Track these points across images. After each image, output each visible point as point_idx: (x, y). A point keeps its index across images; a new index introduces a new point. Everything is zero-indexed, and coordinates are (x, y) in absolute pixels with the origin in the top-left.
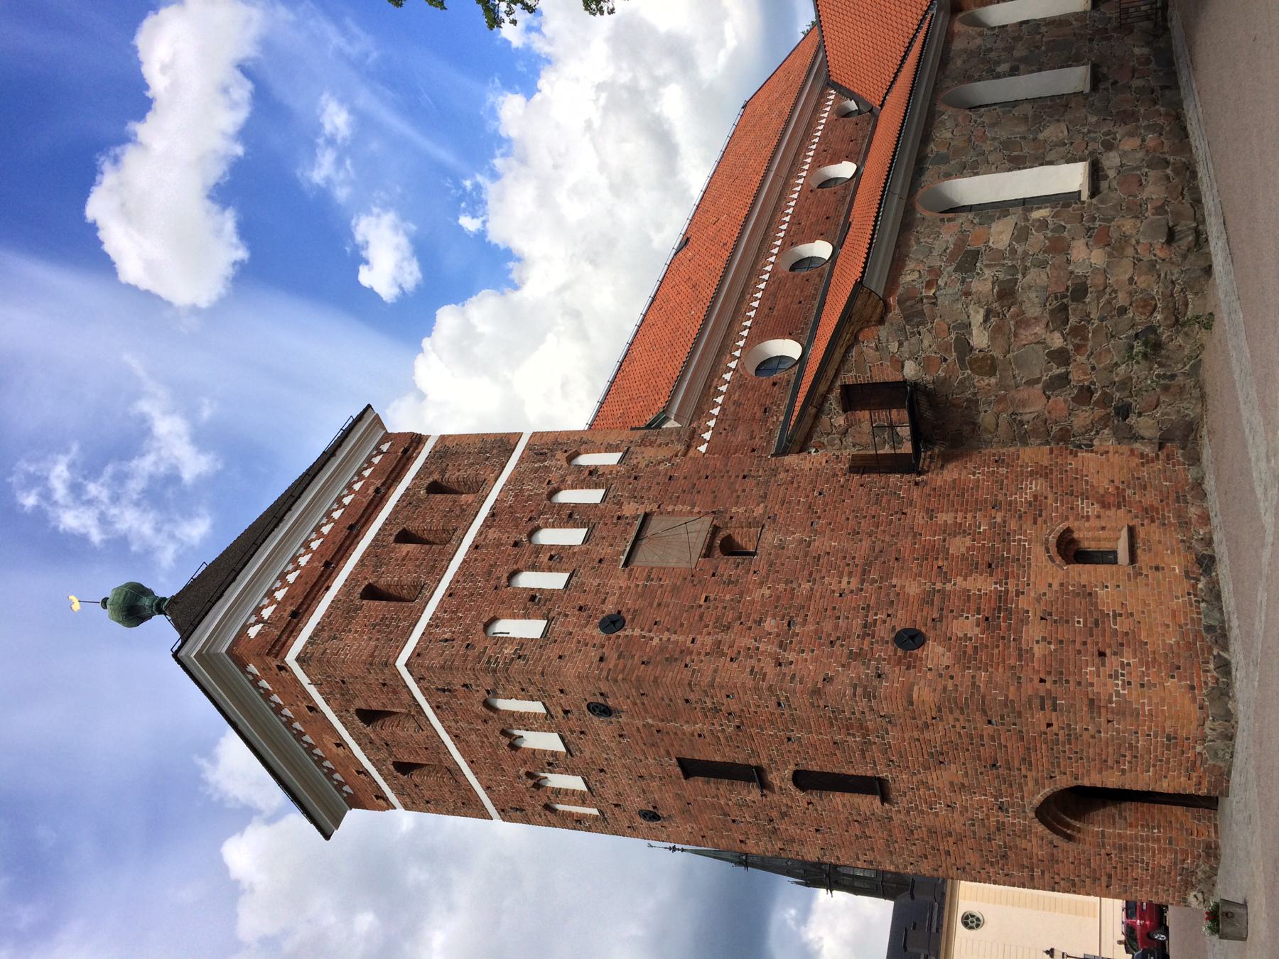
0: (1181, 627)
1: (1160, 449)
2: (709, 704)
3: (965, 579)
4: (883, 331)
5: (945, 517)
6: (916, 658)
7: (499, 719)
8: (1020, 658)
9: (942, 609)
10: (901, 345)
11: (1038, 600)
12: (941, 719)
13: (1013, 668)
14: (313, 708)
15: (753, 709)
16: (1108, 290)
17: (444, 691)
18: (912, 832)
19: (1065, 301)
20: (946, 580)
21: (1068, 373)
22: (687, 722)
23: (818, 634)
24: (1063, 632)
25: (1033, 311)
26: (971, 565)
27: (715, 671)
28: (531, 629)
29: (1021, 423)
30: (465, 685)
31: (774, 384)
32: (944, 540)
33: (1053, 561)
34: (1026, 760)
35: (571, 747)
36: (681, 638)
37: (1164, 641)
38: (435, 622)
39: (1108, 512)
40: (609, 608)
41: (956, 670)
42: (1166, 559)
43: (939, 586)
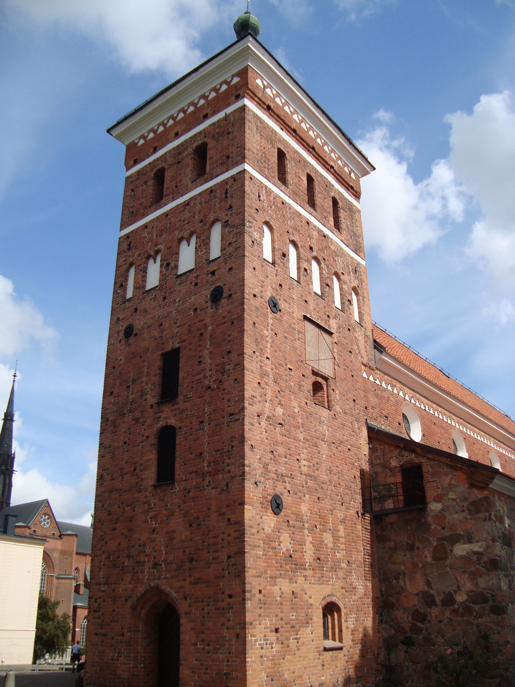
0: (294, 681)
1: (383, 665)
2: (227, 367)
3: (311, 543)
4: (463, 488)
7: (205, 230)
8: (271, 577)
9: (294, 527)
10: (454, 500)
11: (303, 590)
12: (228, 525)
13: (266, 573)
14: (206, 117)
15: (226, 396)
16: (500, 629)
17: (226, 193)
18: (130, 505)
19: (491, 602)
20: (310, 530)
21: (436, 605)
22: (211, 353)
24: (287, 605)
25: (482, 582)
26: (318, 546)
27: (252, 372)
29: (397, 578)
30: (231, 207)
31: (399, 424)
32: (330, 530)
33: (323, 599)
34: (197, 582)
35: (184, 278)
36: (269, 351)
37: (286, 670)
38: (269, 192)
39: (349, 633)
40: (282, 305)
41: (262, 535)
42: (329, 671)
43: (306, 525)
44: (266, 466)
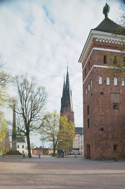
5: (120, 132)
6: (100, 130)
8: (101, 141)
11: (108, 143)
20: (111, 133)
23: (102, 119)
28: (100, 82)
40: (104, 92)
43: (110, 132)
44: (100, 124)
